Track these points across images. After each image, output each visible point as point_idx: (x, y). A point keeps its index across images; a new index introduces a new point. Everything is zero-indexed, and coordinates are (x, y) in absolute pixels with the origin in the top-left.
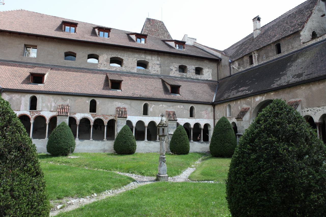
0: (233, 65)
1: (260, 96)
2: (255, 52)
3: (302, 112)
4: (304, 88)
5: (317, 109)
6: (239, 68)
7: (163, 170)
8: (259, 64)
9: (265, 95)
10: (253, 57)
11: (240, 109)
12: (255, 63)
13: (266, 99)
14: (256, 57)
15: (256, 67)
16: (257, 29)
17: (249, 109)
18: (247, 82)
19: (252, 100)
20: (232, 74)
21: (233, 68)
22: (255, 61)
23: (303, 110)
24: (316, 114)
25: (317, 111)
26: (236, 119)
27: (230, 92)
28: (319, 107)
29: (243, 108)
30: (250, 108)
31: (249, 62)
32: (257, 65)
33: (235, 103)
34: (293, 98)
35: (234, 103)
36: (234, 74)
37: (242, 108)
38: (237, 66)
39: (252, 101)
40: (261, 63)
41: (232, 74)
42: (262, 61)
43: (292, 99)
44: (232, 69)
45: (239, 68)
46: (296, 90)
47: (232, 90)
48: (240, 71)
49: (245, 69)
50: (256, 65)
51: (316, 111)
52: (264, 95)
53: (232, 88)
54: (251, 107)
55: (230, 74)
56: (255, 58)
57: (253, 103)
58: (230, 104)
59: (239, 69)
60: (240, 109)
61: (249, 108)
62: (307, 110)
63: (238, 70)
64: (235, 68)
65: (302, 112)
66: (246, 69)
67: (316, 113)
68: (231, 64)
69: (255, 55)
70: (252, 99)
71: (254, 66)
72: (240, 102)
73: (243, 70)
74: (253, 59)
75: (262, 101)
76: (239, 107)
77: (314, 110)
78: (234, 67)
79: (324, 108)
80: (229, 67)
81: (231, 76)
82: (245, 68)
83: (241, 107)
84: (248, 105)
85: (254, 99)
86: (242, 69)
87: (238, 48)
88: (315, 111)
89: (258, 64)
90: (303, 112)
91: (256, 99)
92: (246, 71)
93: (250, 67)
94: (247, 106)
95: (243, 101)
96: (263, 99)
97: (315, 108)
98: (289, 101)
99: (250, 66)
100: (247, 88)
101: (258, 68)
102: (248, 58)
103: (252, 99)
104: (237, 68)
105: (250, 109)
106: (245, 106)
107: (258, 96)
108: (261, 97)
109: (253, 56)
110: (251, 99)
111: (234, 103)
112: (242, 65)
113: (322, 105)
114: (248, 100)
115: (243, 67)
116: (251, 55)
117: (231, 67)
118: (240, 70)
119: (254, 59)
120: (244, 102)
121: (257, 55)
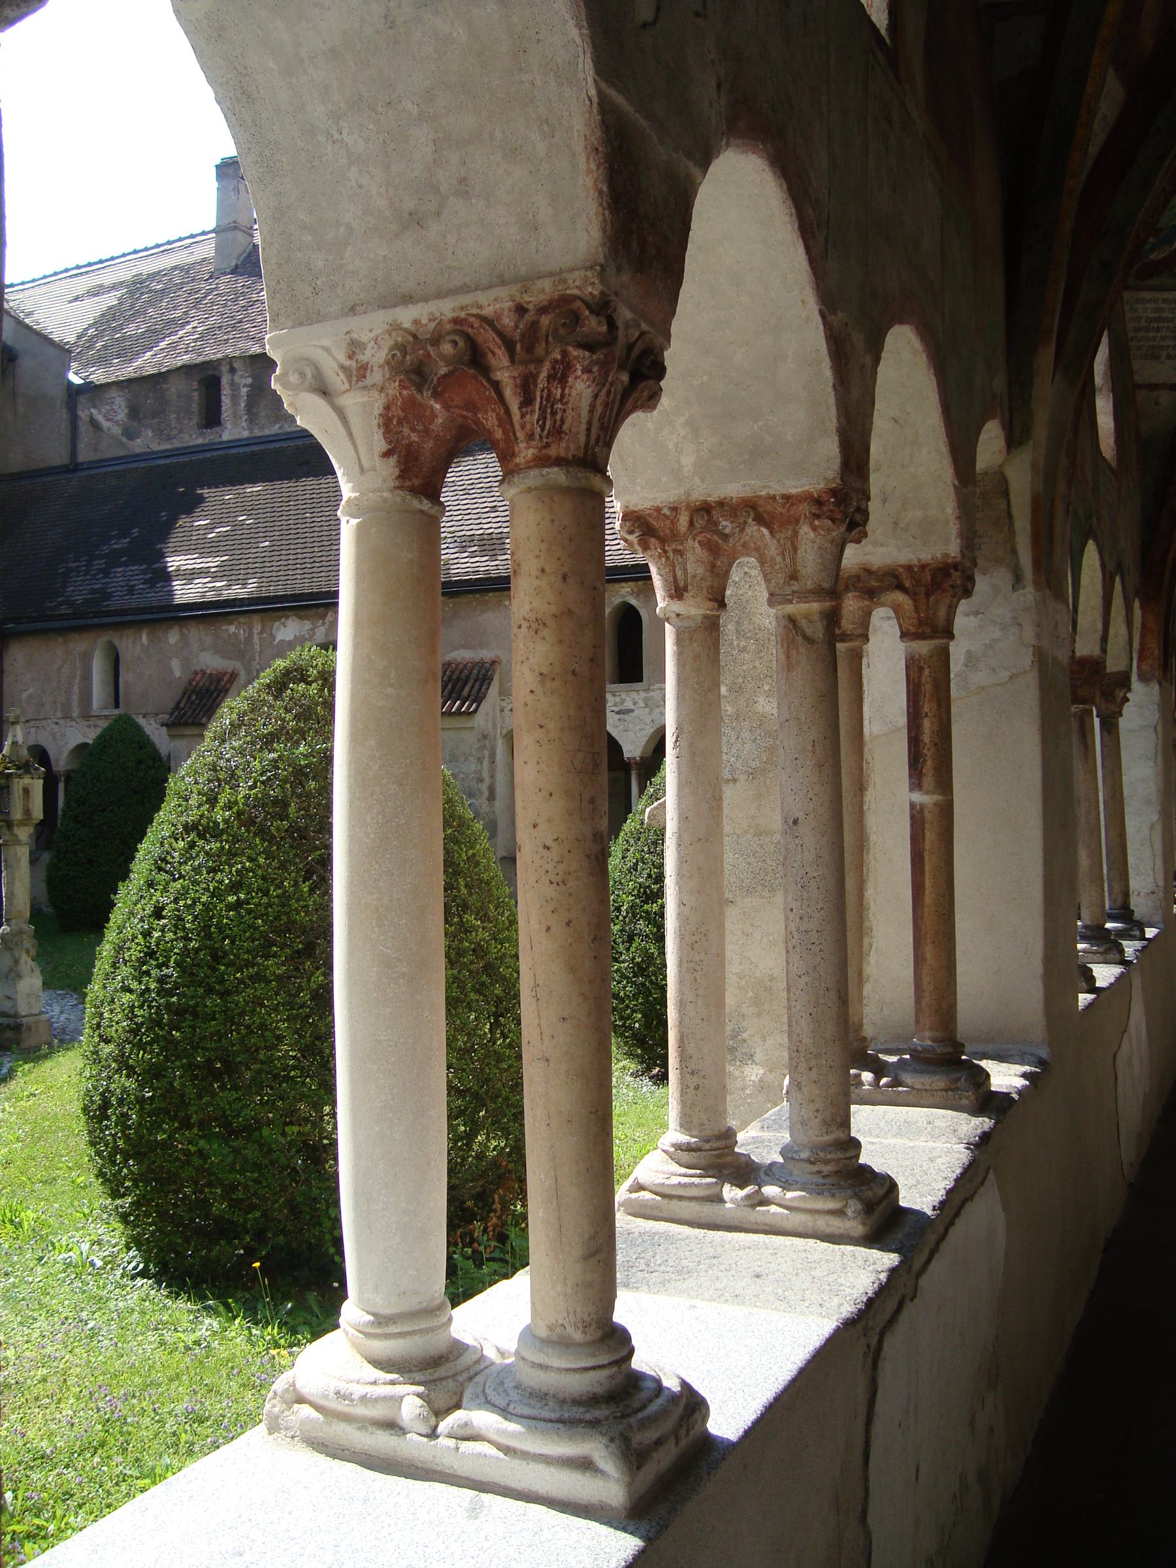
0: (94, 407)
1: (301, 618)
2: (236, 365)
3: (502, 711)
6: (130, 434)
7: (28, 995)
8: (257, 433)
10: (226, 391)
11: (177, 673)
12: (235, 425)
14: (244, 391)
15: (236, 444)
16: (236, 228)
18: (199, 528)
19: (255, 631)
20: (81, 458)
21: (94, 423)
22: (235, 415)
23: (504, 704)
26: (165, 729)
27: (106, 572)
29: (198, 668)
30: (242, 673)
31: (195, 407)
32: (246, 434)
33: (148, 635)
34: (465, 646)
35: (144, 637)
36: (96, 458)
37: (196, 673)
38: (122, 415)
39: (256, 639)
40: (267, 432)
41: (81, 458)
42: (275, 423)
43: (462, 651)
44: (84, 428)
45: (130, 434)
47: (113, 559)
48: (138, 451)
49: (168, 447)
50: (236, 437)
52: (326, 615)
53: (105, 550)
55: (74, 454)
56: (235, 398)
57: (257, 647)
58: (117, 643)
59: (131, 438)
60: (177, 673)
61: (237, 675)
63: (124, 440)
64: (105, 424)
65: (502, 711)
66: (177, 444)
68: (82, 400)
69: (237, 379)
70: (257, 628)
71: (226, 437)
72: (182, 635)
73: (155, 447)
74: (223, 398)
78: (100, 418)
80: (64, 414)
81: (75, 471)
82: (169, 438)
86: (147, 442)
87: (110, 300)
89: (251, 430)
90: (507, 712)
91: (278, 629)
92: (175, 460)
93: (200, 441)
96: (314, 634)
98: (449, 657)
99: (202, 434)
100: (212, 563)
101: (253, 453)
102: (195, 385)
103: (257, 628)
104: (117, 431)
106: (211, 661)
107: (287, 618)
108: (307, 625)
109: (225, 380)
110: (251, 628)
111: (144, 637)
112: (155, 421)
114: (232, 629)
115: (161, 431)
116: (216, 373)
117: (83, 414)
118: (137, 446)
119: (226, 402)
120: (208, 640)
121: (249, 381)
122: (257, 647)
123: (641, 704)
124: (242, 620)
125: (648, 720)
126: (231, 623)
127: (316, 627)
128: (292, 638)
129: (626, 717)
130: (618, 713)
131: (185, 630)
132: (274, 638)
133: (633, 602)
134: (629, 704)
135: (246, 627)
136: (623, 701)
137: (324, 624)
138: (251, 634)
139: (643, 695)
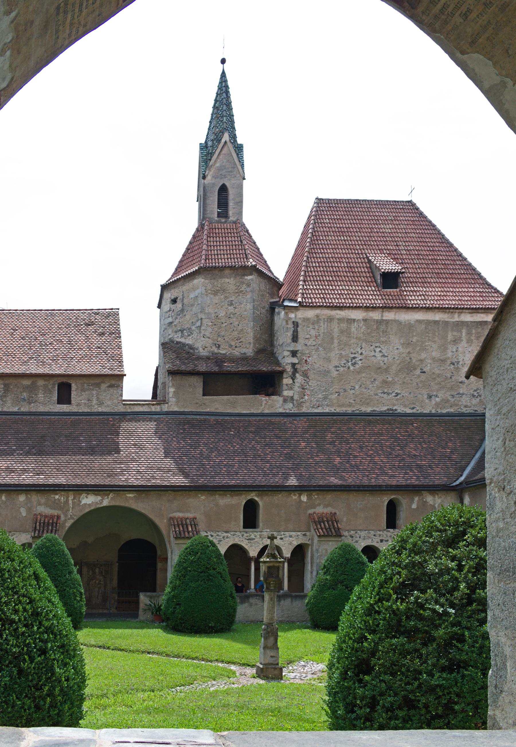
1: (96, 495)
4: (203, 497)
5: (223, 535)
9: (111, 495)
13: (113, 503)
17: (58, 517)
19: (70, 498)
24: (221, 543)
25: (224, 537)
28: (227, 532)
29: (37, 513)
33: (6, 497)
35: (3, 498)
39: (70, 502)
46: (188, 498)
51: (221, 537)
52: (109, 494)
54: (66, 515)
62: (206, 534)
67: (221, 541)
70: (71, 498)
72: (27, 497)
75: (102, 506)
76: (23, 512)
77: (218, 535)
79: (235, 534)
83: (29, 510)
84: (55, 509)
85: (77, 498)
88: (219, 537)
91: (83, 498)
94: (49, 510)
95: (35, 498)
96: (103, 502)
97: (220, 534)
98: (172, 515)
103: (71, 498)
105: (63, 518)
107: (88, 494)
108: (99, 498)
111: (3, 498)
113: (233, 530)
114: (57, 497)
122: (71, 506)
123: (258, 537)
124: (63, 493)
125: (261, 543)
126: (57, 494)
127: (103, 499)
128: (90, 502)
129: (252, 541)
130: (248, 540)
131: (29, 496)
132: (81, 502)
133: (256, 499)
134: (253, 536)
135: (65, 497)
136: (250, 535)
137: (108, 498)
138: (67, 500)
139: (259, 533)
